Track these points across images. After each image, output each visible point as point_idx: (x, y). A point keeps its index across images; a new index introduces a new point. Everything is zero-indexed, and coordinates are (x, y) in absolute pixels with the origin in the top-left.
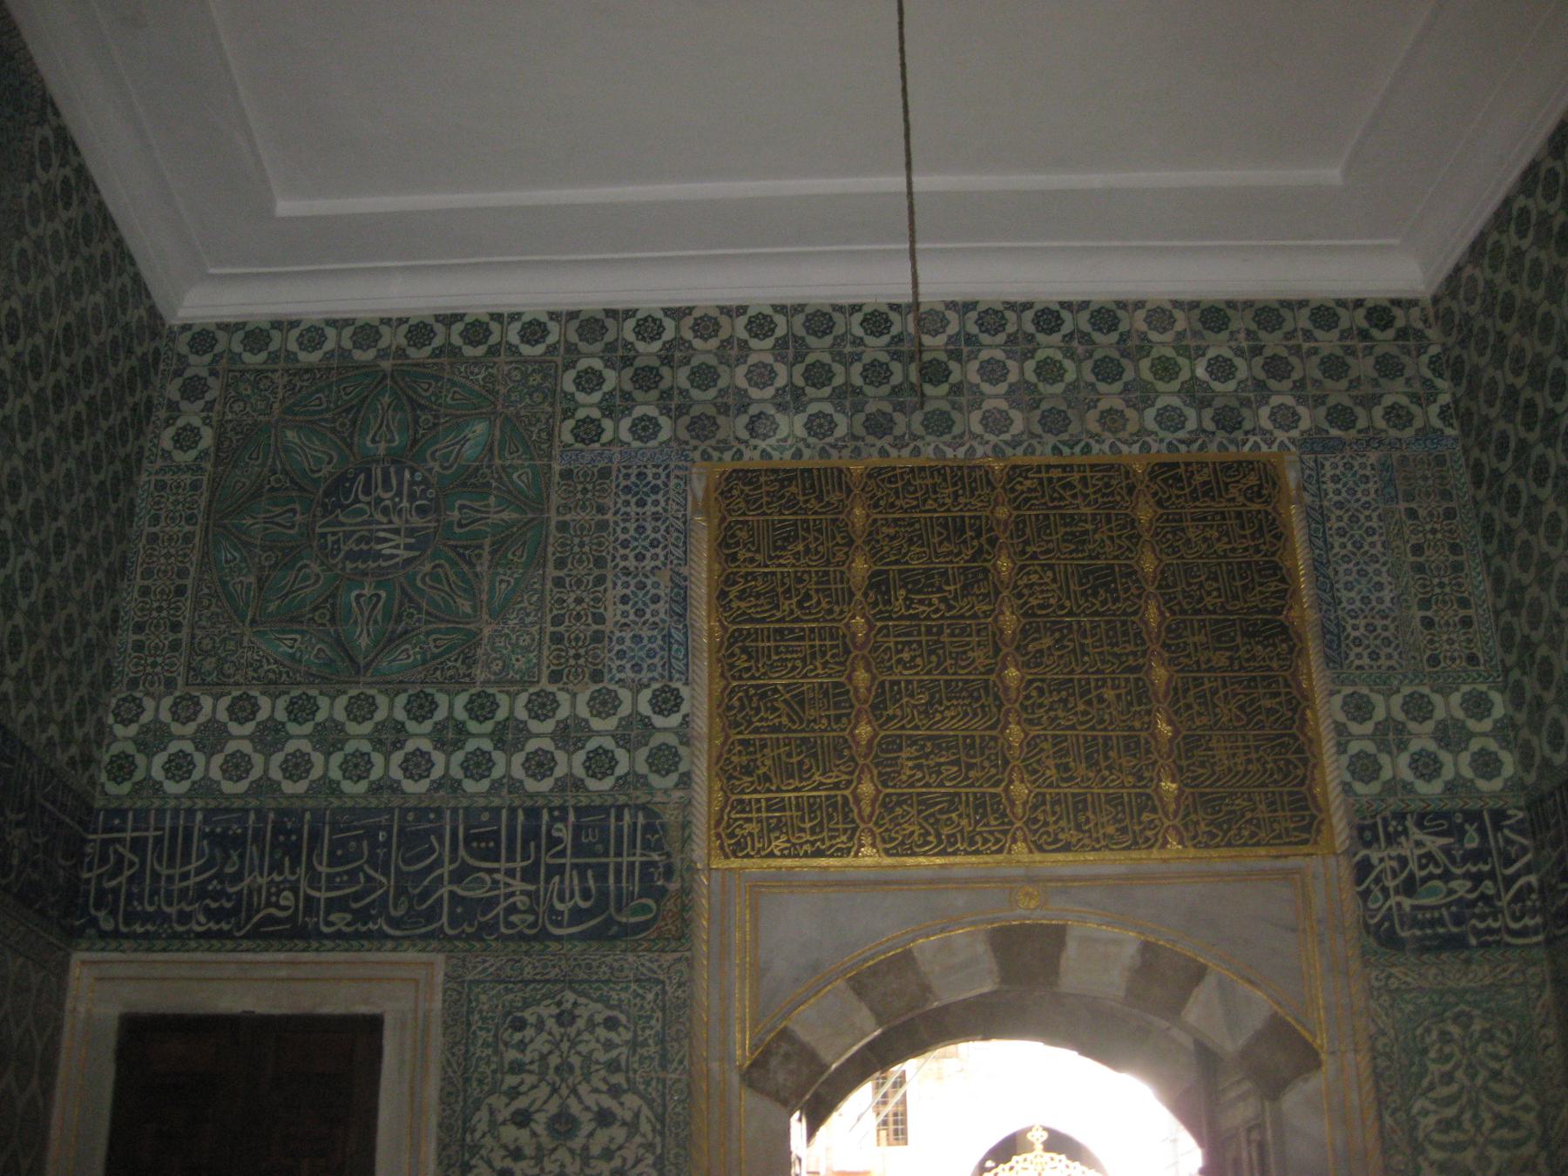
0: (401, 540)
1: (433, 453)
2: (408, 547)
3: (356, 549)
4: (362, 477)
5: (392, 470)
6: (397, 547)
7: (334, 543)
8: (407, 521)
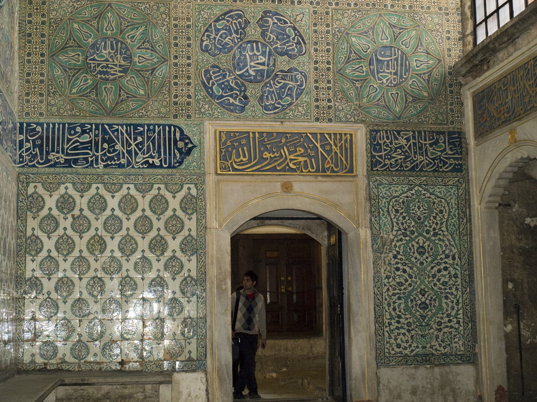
0: (117, 69)
1: (128, 37)
2: (120, 72)
3: (101, 70)
4: (103, 43)
5: (114, 42)
6: (116, 71)
7: (94, 67)
8: (120, 62)
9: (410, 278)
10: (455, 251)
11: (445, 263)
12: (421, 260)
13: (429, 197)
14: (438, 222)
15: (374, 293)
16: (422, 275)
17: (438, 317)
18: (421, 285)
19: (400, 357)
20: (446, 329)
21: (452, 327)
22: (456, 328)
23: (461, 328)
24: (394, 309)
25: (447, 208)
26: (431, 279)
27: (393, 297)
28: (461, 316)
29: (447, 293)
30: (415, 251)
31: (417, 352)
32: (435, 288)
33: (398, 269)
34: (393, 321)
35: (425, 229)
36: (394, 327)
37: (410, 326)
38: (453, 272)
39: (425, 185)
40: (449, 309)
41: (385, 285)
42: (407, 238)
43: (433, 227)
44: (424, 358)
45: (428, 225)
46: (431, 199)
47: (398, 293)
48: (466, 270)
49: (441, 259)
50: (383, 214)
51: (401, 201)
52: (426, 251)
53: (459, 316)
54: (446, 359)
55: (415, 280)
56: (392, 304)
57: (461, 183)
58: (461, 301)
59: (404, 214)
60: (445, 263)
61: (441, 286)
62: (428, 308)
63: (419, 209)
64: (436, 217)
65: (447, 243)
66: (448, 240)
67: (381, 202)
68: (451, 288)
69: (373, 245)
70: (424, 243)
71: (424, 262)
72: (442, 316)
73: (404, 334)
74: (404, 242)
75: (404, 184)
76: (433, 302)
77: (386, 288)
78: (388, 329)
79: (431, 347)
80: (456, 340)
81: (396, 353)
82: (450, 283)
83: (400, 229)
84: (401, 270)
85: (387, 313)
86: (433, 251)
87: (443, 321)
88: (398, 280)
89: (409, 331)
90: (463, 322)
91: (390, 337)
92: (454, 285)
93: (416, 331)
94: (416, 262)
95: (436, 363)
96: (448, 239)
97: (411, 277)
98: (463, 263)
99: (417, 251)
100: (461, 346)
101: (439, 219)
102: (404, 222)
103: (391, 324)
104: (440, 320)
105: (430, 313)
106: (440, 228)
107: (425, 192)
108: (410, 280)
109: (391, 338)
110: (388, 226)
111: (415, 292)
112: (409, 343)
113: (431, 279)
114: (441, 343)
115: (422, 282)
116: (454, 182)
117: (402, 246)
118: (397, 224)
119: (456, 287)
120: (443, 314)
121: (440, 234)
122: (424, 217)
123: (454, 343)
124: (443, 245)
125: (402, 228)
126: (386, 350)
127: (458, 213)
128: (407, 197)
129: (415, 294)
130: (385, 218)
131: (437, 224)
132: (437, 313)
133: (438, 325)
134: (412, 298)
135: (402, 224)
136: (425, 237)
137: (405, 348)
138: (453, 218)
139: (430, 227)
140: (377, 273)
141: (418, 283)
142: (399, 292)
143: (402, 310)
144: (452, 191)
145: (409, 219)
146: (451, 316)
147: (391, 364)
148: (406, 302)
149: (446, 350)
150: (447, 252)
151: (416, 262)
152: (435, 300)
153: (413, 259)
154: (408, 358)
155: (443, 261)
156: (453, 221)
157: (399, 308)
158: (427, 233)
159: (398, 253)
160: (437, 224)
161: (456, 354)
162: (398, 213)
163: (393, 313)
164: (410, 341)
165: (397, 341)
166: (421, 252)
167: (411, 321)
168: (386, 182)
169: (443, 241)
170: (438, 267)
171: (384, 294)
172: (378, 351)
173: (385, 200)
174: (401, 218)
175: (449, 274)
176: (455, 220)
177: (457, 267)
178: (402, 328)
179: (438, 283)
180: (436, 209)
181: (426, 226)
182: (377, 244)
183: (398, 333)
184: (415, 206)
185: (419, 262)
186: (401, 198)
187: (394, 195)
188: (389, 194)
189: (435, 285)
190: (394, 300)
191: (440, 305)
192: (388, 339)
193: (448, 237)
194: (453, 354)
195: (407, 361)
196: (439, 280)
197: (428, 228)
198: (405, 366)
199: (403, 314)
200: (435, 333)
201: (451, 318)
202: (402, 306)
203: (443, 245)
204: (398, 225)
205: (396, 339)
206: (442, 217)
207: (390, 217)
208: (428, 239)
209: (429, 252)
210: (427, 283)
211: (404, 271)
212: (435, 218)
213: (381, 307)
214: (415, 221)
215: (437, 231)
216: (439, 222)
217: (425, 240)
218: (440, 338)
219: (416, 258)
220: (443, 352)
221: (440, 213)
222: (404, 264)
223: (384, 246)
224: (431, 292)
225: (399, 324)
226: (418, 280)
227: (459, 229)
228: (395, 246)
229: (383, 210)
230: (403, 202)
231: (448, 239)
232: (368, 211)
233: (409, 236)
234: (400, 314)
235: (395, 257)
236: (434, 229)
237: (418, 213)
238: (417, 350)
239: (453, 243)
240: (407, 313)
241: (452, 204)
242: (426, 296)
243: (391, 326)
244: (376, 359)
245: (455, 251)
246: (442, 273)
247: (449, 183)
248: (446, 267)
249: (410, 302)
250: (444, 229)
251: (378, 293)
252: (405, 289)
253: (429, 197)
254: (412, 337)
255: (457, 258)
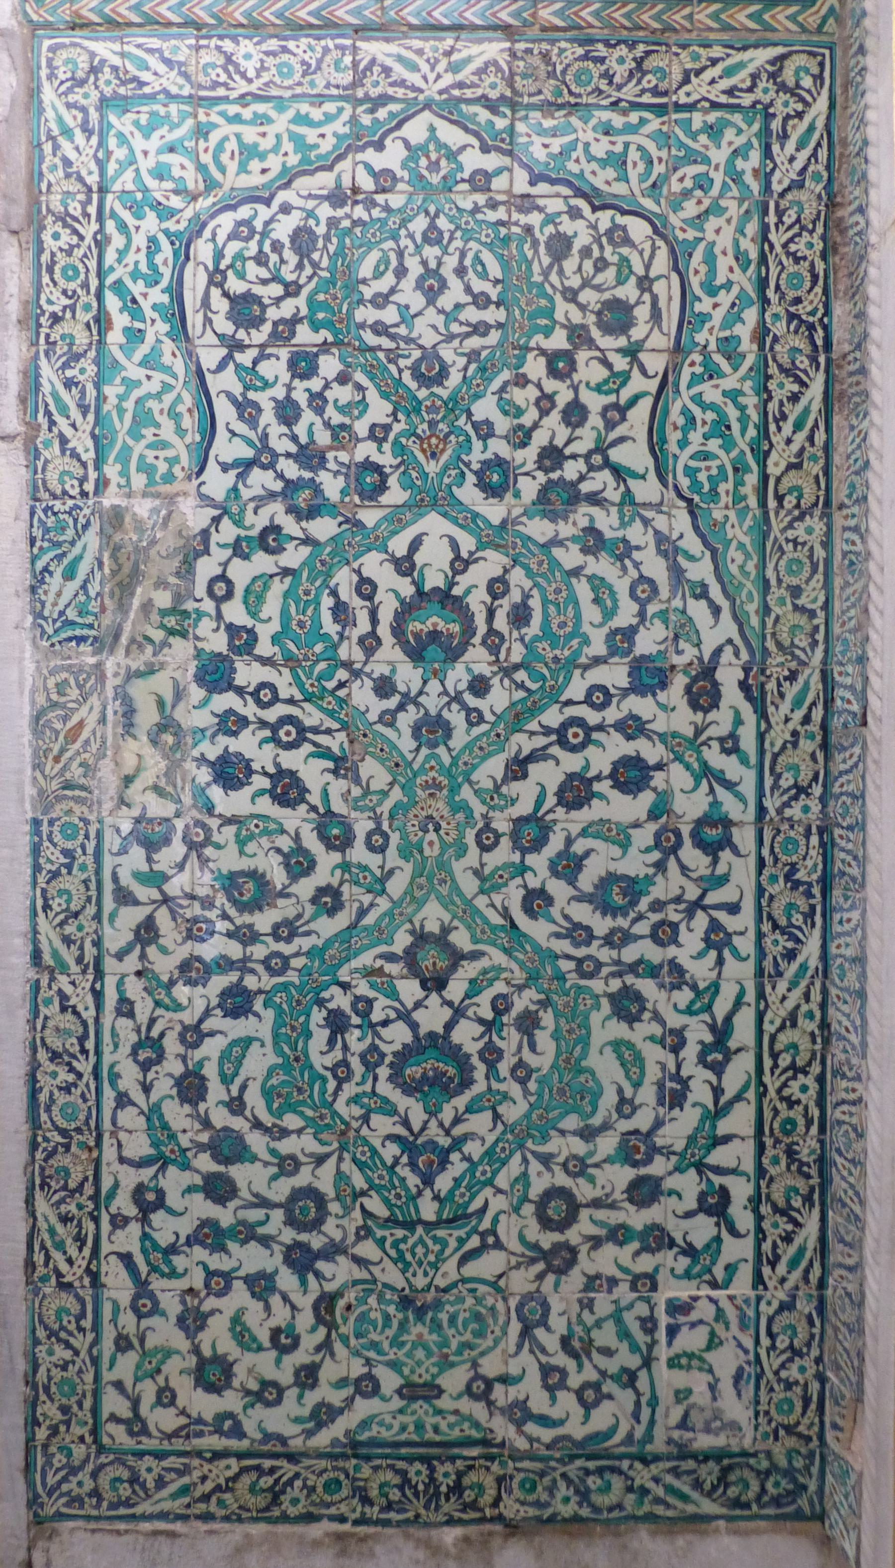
9: (329, 844)
10: (715, 632)
11: (632, 727)
12: (432, 702)
13: (526, 203)
14: (589, 398)
15: (36, 956)
16: (431, 823)
17: (546, 1160)
18: (421, 904)
19: (217, 1455)
20: (610, 1250)
21: (657, 1239)
22: (690, 1251)
23: (738, 1249)
24: (191, 1087)
25: (667, 290)
26: (503, 854)
27: (182, 992)
28: (738, 1153)
29: (634, 968)
30: (384, 631)
31: (365, 1424)
32: (538, 930)
33: (230, 772)
34: (174, 1181)
35: (477, 455)
36: (185, 1227)
37: (316, 1224)
38: (691, 805)
39: (492, 107)
40: (647, 1094)
41: (124, 897)
42: (324, 528)
43: (540, 438)
44: (417, 1472)
45: (502, 424)
46: (535, 219)
47: (225, 964)
48: (801, 790)
49: (598, 697)
50: (135, 336)
51: (283, 229)
52: (469, 630)
53: (720, 1156)
54: (593, 1482)
55: (373, 861)
56: (172, 1045)
57: (794, 91)
58: (743, 1030)
59: (304, 335)
60: (632, 727)
61: (582, 913)
62: (467, 1083)
63: (432, 295)
64: (568, 356)
65: (655, 567)
66: (667, 547)
67: (118, 241)
68: (665, 933)
69: (39, 579)
70: (461, 563)
71: (456, 717)
72: (579, 1146)
73: (261, 1285)
74: (294, 556)
75: (319, 100)
76: (510, 1040)
77: (131, 917)
78: (129, 1239)
79: (481, 1389)
80: (691, 1340)
81: (194, 1425)
82: (658, 891)
83: (263, 457)
84: (260, 782)
85: (128, 1117)
86: (534, 628)
87: (584, 1191)
88: (229, 860)
89: (301, 1260)
90: (755, 1202)
91: (144, 1303)
92: (698, 905)
93: (359, 1261)
94: (388, 719)
95: (510, 1508)
96: (660, 538)
97: (335, 833)
98: (779, 735)
99: (398, 631)
100: (726, 1386)
101: (598, 373)
102: (300, 397)
103: (160, 1202)
104: (562, 1179)
105: (480, 1123)
106: (601, 449)
107: (491, 162)
108: (327, 863)
109: (156, 1310)
110: (167, 431)
111: (366, 959)
112: (301, 1357)
113: (503, 854)
114: (561, 1360)
115: (431, 878)
116: (741, 78)
117: (278, 587)
118: (247, 410)
119: (715, 926)
120: (588, 1134)
121: (595, 499)
122: (473, 356)
123: (673, 1363)
124: (622, 587)
125: (282, 445)
126: (114, 1403)
127: (761, 333)
128: (336, 198)
129: (370, 973)
130: (145, 363)
131: (575, 414)
132: (538, 1126)
133: (546, 1223)
134: (341, 1001)
135: (287, 412)
136: (470, 520)
137: (267, 1393)
138: (712, 373)
139: (521, 437)
140: (61, 791)
141: (397, 886)
142: (235, 950)
143: (254, 1099)
144: (719, 156)
145: (343, 379)
146: (655, 1150)
147: (144, 1507)
148: (290, 1037)
149: (601, 1418)
150: (646, 643)
151: (388, 719)
152: (528, 1024)
153: (362, 695)
154: (288, 1469)
155: (612, 714)
156: (711, 393)
157: (227, 1080)
158: (493, 491)
159: (243, 640)
160: (575, 414)
161: (684, 1453)
162: (256, 322)
163: (177, 1115)
164: (309, 1341)
165: (205, 1339)
166: (434, 635)
167: (326, 1186)
168: (172, 81)
169: (623, 552)
170: (572, 762)
171: (110, 964)
172: (50, 1410)
173: (150, 223)
174: (275, 368)
175: (653, 815)
176: (729, 383)
177: (731, 767)
178: (247, 1233)
179: (558, 889)
180: (571, 295)
181: (485, 431)
182: (69, 576)
183: (210, 1274)
184: (401, 272)
185: (407, 719)
186: (286, 209)
187: (234, 179)
188: (192, 179)
189: (536, 901)
190: (188, 1018)
191: (571, 1062)
192: (128, 1321)
193: (661, 522)
194: (658, 1445)
195: (276, 1495)
196: (568, 866)
197: (499, 447)
198: (258, 1529)
199: (257, 1124)
200: (521, 1282)
201: (658, 1167)
202: (258, 1063)
203: (622, 587)
204: (252, 422)
205: (193, 1321)
206: (620, 363)
207: (190, 354)
208: (498, 536)
209: (494, 641)
210: (469, 885)
211: (287, 789)
212: (560, 365)
213: (85, 1066)
214: (391, 390)
215: (571, 470)
216: (594, 402)
217: (467, 543)
218: (558, 1324)
219: (384, 687)
220: (576, 1430)
221: (607, 329)
222: (287, 733)
223: (124, 588)
224: (498, 957)
225: (221, 1201)
226: (392, 857)
227: (763, 458)
228: (222, 588)
229: (132, 305)
230: (303, 240)
231: (660, 538)
232: (14, 308)
233: (333, 510)
234: (238, 1124)
235: (215, 675)
236: (552, 456)
237: (420, 326)
238: (363, 1407)
239: (701, 570)
240: (292, 1121)
241: (710, 259)
242: (456, 989)
243: (158, 1218)
244: (28, 1467)
245: (715, 632)
246: (595, 811)
247: (699, 88)
248: (635, 762)
249: (321, 1036)
250: (634, 455)
251: (69, 956)
252: (286, 930)
253: (526, 203)
254: (325, 1306)
255: (731, 695)
